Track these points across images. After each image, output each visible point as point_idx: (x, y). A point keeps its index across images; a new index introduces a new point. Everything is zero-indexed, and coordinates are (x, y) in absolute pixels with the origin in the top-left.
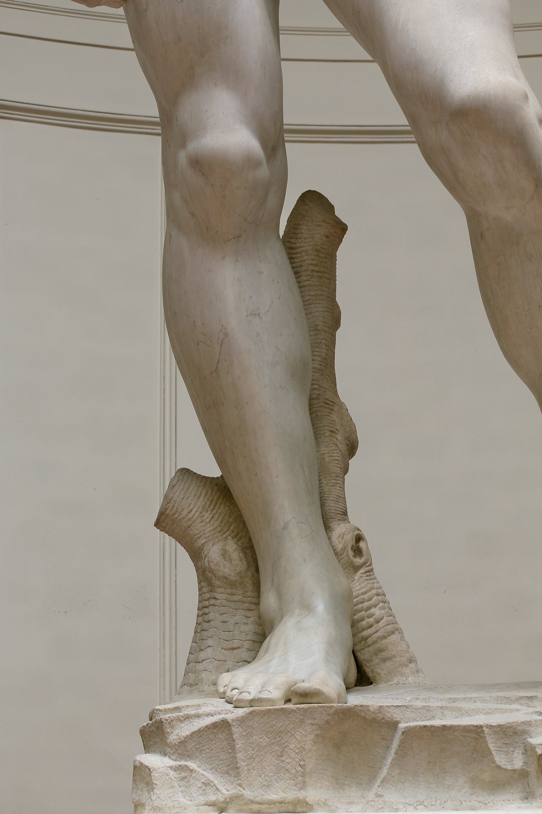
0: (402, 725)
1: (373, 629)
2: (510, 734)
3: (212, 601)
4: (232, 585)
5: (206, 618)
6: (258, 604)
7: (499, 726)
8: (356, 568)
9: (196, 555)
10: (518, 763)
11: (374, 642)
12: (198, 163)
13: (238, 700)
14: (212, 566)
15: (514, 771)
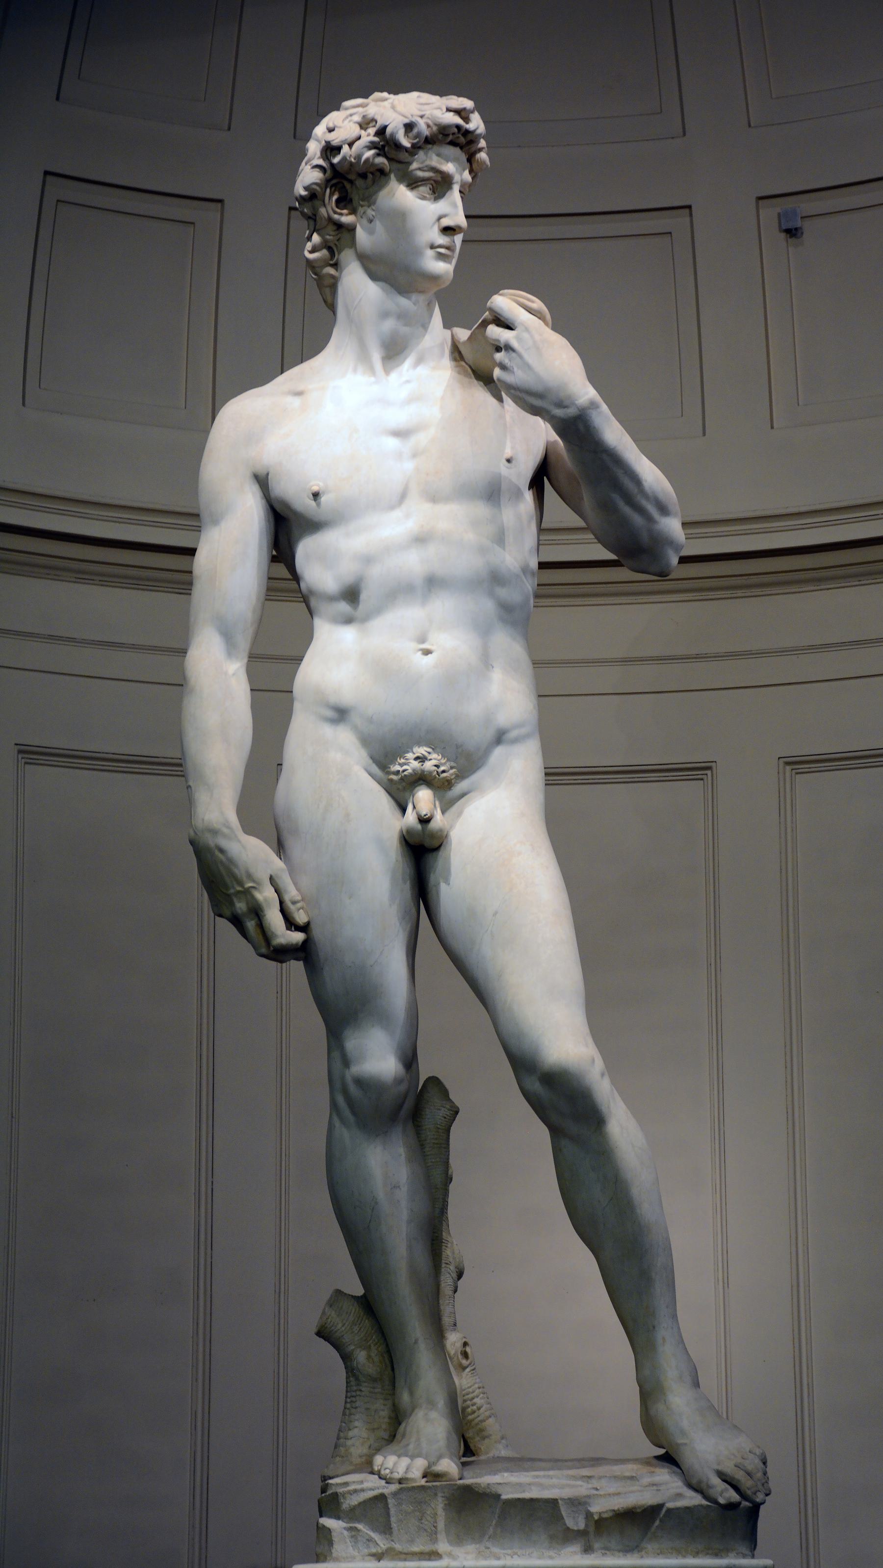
0: (504, 1497)
1: (476, 1414)
2: (576, 1503)
3: (358, 1393)
4: (374, 1380)
5: (354, 1405)
6: (394, 1394)
7: (569, 1499)
8: (464, 1368)
9: (346, 1357)
10: (582, 1526)
11: (477, 1424)
12: (360, 1082)
13: (390, 1478)
14: (359, 1367)
15: (578, 1531)
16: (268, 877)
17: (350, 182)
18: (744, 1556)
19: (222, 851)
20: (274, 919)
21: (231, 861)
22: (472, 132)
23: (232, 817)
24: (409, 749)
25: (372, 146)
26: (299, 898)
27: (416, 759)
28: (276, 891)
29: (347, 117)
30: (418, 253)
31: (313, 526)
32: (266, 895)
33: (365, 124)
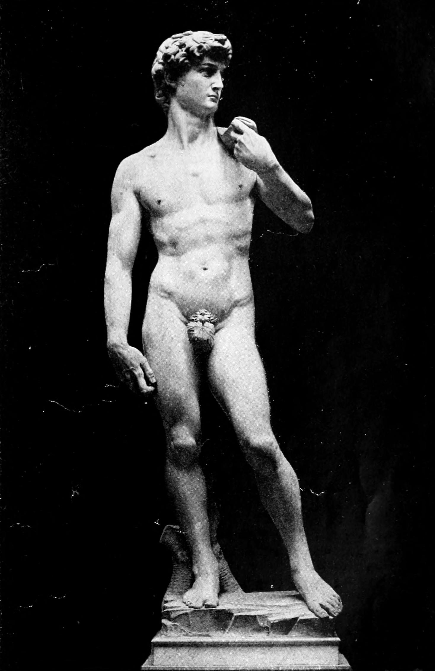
0: (235, 614)
16: (139, 364)
17: (176, 70)
18: (330, 637)
19: (120, 353)
20: (142, 382)
21: (124, 358)
22: (225, 49)
23: (125, 340)
24: (198, 310)
25: (183, 56)
26: (152, 372)
27: (201, 314)
28: (144, 370)
29: (173, 43)
30: (204, 99)
31: (159, 214)
32: (139, 371)
33: (181, 46)
